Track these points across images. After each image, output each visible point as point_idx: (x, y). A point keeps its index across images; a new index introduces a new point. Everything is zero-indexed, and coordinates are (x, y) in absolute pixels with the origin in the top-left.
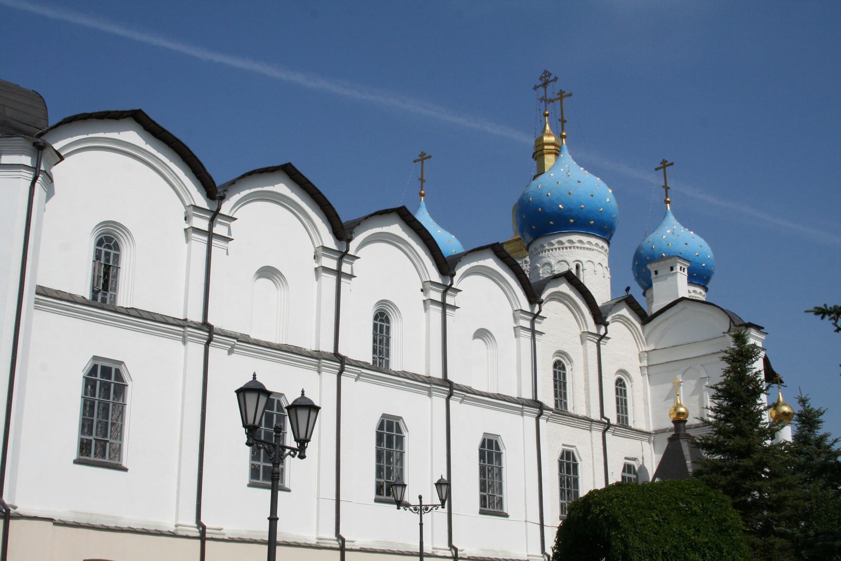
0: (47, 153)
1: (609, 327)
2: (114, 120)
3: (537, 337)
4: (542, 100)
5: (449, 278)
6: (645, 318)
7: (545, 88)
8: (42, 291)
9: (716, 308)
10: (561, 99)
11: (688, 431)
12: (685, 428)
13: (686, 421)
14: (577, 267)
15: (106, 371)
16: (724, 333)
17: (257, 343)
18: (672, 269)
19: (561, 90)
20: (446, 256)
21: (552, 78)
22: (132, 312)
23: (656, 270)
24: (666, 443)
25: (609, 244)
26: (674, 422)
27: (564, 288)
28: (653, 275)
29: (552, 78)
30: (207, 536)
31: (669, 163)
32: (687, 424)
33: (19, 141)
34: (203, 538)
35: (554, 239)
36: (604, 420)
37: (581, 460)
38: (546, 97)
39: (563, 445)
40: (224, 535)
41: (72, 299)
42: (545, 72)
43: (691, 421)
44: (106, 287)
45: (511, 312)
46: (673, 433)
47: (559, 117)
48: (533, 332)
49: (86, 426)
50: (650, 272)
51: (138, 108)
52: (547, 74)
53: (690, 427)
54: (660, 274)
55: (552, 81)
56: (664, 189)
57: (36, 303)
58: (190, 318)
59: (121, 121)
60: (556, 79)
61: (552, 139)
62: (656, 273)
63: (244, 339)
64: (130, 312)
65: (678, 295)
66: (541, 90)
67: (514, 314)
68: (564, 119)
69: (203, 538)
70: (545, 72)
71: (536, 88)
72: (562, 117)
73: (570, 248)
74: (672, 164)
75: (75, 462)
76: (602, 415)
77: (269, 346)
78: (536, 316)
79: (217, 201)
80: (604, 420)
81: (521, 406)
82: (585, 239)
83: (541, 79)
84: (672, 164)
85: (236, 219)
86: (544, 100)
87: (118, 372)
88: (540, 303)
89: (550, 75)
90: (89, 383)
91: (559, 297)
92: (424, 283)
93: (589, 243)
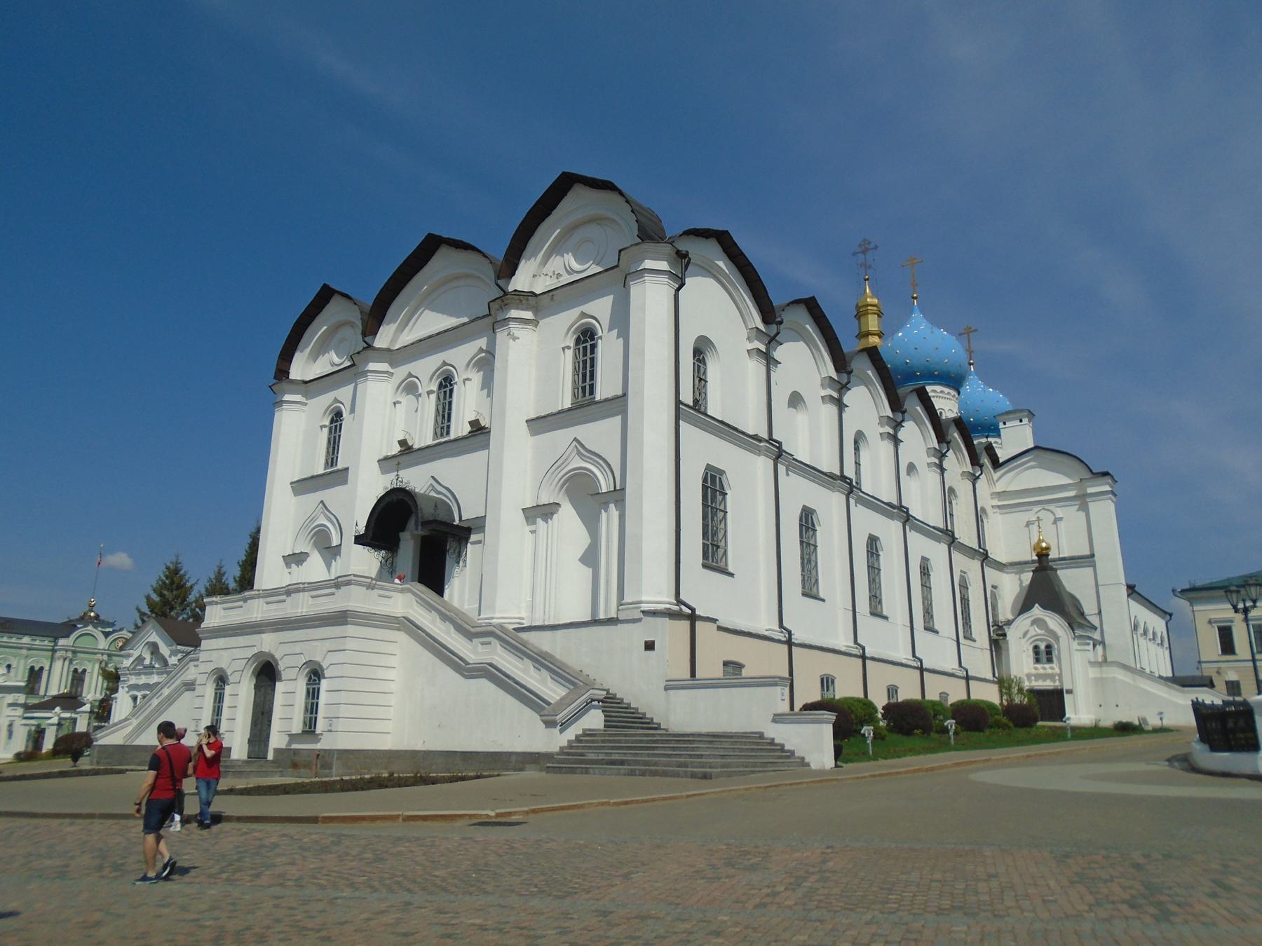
2: (704, 239)
4: (861, 265)
5: (901, 415)
6: (996, 464)
7: (865, 254)
12: (1048, 561)
13: (1048, 555)
18: (1021, 421)
21: (871, 247)
24: (1032, 573)
25: (959, 393)
26: (1037, 555)
28: (1001, 425)
29: (871, 247)
31: (973, 329)
32: (1050, 557)
33: (667, 248)
36: (981, 550)
37: (970, 585)
42: (864, 240)
45: (925, 450)
46: (1037, 565)
51: (726, 229)
53: (1054, 560)
55: (872, 249)
59: (709, 239)
60: (876, 247)
61: (875, 301)
62: (1005, 423)
66: (861, 256)
69: (790, 643)
70: (864, 240)
71: (854, 254)
74: (975, 331)
76: (980, 547)
80: (981, 550)
81: (940, 534)
82: (946, 390)
83: (860, 246)
84: (975, 331)
89: (870, 243)
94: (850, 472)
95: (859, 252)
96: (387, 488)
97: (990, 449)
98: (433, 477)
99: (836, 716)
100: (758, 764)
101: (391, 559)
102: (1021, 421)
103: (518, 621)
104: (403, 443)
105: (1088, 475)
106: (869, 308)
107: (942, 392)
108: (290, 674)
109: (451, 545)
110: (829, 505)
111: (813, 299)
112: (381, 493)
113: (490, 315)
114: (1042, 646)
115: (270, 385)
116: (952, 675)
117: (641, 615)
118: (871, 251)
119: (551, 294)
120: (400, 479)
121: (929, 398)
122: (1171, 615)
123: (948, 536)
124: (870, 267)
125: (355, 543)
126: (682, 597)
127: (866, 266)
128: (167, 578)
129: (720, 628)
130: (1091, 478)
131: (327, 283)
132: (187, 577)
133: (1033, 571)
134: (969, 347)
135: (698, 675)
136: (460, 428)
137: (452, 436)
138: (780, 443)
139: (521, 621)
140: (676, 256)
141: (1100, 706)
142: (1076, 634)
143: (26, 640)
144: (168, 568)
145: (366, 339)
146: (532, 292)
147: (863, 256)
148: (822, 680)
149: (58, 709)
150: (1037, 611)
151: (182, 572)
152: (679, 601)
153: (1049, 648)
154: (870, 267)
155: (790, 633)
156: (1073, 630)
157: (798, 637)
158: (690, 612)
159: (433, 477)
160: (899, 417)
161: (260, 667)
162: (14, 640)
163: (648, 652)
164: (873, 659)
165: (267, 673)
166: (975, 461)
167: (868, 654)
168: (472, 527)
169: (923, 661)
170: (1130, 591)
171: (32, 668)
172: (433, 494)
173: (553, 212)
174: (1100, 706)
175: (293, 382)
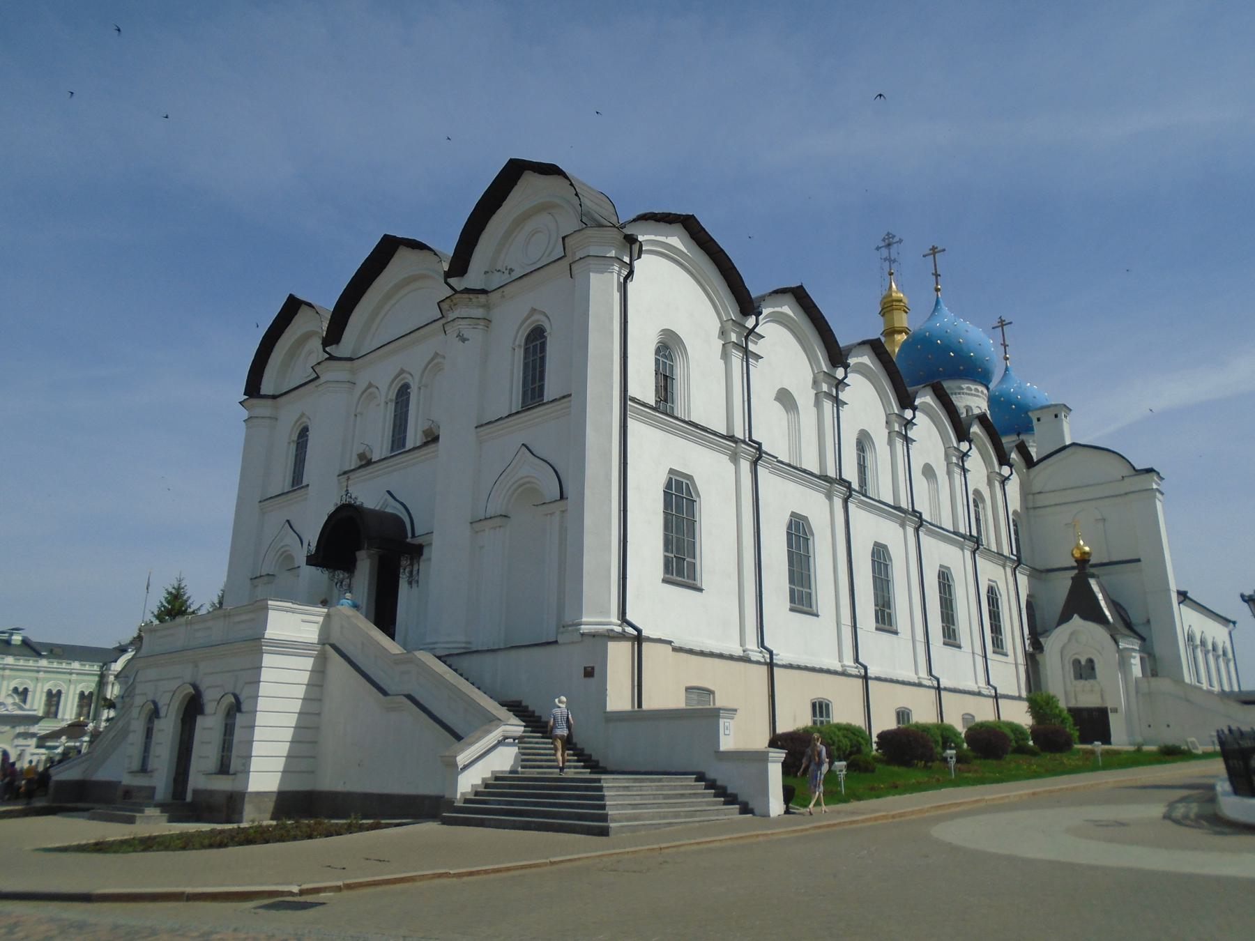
0: (636, 248)
2: (668, 225)
4: (885, 260)
6: (1030, 463)
7: (889, 249)
9: (1112, 454)
10: (934, 254)
11: (1092, 570)
13: (1089, 561)
16: (1123, 477)
19: (933, 246)
23: (1039, 417)
25: (988, 389)
28: (1035, 421)
29: (894, 241)
30: (775, 661)
31: (1006, 322)
32: (1091, 563)
34: (771, 665)
35: (964, 384)
37: (1001, 596)
38: (890, 256)
39: (989, 580)
40: (782, 660)
42: (888, 234)
43: (1093, 561)
47: (934, 272)
50: (1032, 421)
52: (891, 236)
54: (1042, 420)
55: (895, 243)
56: (1003, 347)
59: (673, 225)
60: (900, 241)
65: (1065, 442)
66: (885, 252)
67: (946, 451)
68: (938, 273)
69: (771, 665)
70: (888, 234)
71: (878, 248)
72: (936, 272)
73: (959, 394)
74: (1010, 323)
79: (754, 317)
83: (884, 240)
84: (1010, 323)
85: (764, 337)
86: (889, 260)
89: (894, 236)
92: (888, 416)
94: (850, 474)
95: (882, 247)
96: (337, 505)
97: (1023, 450)
98: (389, 492)
99: (786, 754)
100: (682, 814)
101: (348, 580)
102: (1056, 416)
103: (463, 645)
104: (362, 456)
105: (1129, 472)
106: (894, 303)
108: (209, 707)
109: (404, 562)
111: (801, 288)
112: (332, 509)
113: (443, 317)
114: (1083, 663)
115: (240, 400)
116: (979, 694)
118: (895, 245)
119: (501, 290)
120: (349, 495)
122: (1234, 623)
123: (975, 543)
124: (894, 261)
125: (307, 564)
126: (629, 617)
127: (891, 261)
128: (168, 602)
129: (676, 649)
130: (1135, 475)
131: (293, 293)
132: (188, 603)
133: (1072, 578)
134: (1004, 340)
135: (645, 706)
136: (413, 437)
137: (407, 449)
138: (760, 444)
139: (468, 646)
140: (624, 241)
141: (1150, 726)
142: (1121, 647)
143: (76, 665)
144: (170, 593)
145: (327, 349)
146: (483, 289)
147: (887, 251)
148: (814, 705)
149: (64, 739)
150: (1076, 619)
151: (185, 598)
153: (1091, 661)
154: (894, 261)
155: (771, 653)
156: (1117, 643)
157: (782, 656)
158: (636, 633)
159: (389, 492)
161: (186, 703)
162: (64, 665)
163: (587, 679)
164: (878, 679)
165: (193, 707)
166: (1003, 460)
167: (872, 672)
168: (424, 544)
169: (941, 680)
170: (1182, 598)
171: (82, 694)
172: (389, 510)
173: (504, 204)
174: (1150, 726)
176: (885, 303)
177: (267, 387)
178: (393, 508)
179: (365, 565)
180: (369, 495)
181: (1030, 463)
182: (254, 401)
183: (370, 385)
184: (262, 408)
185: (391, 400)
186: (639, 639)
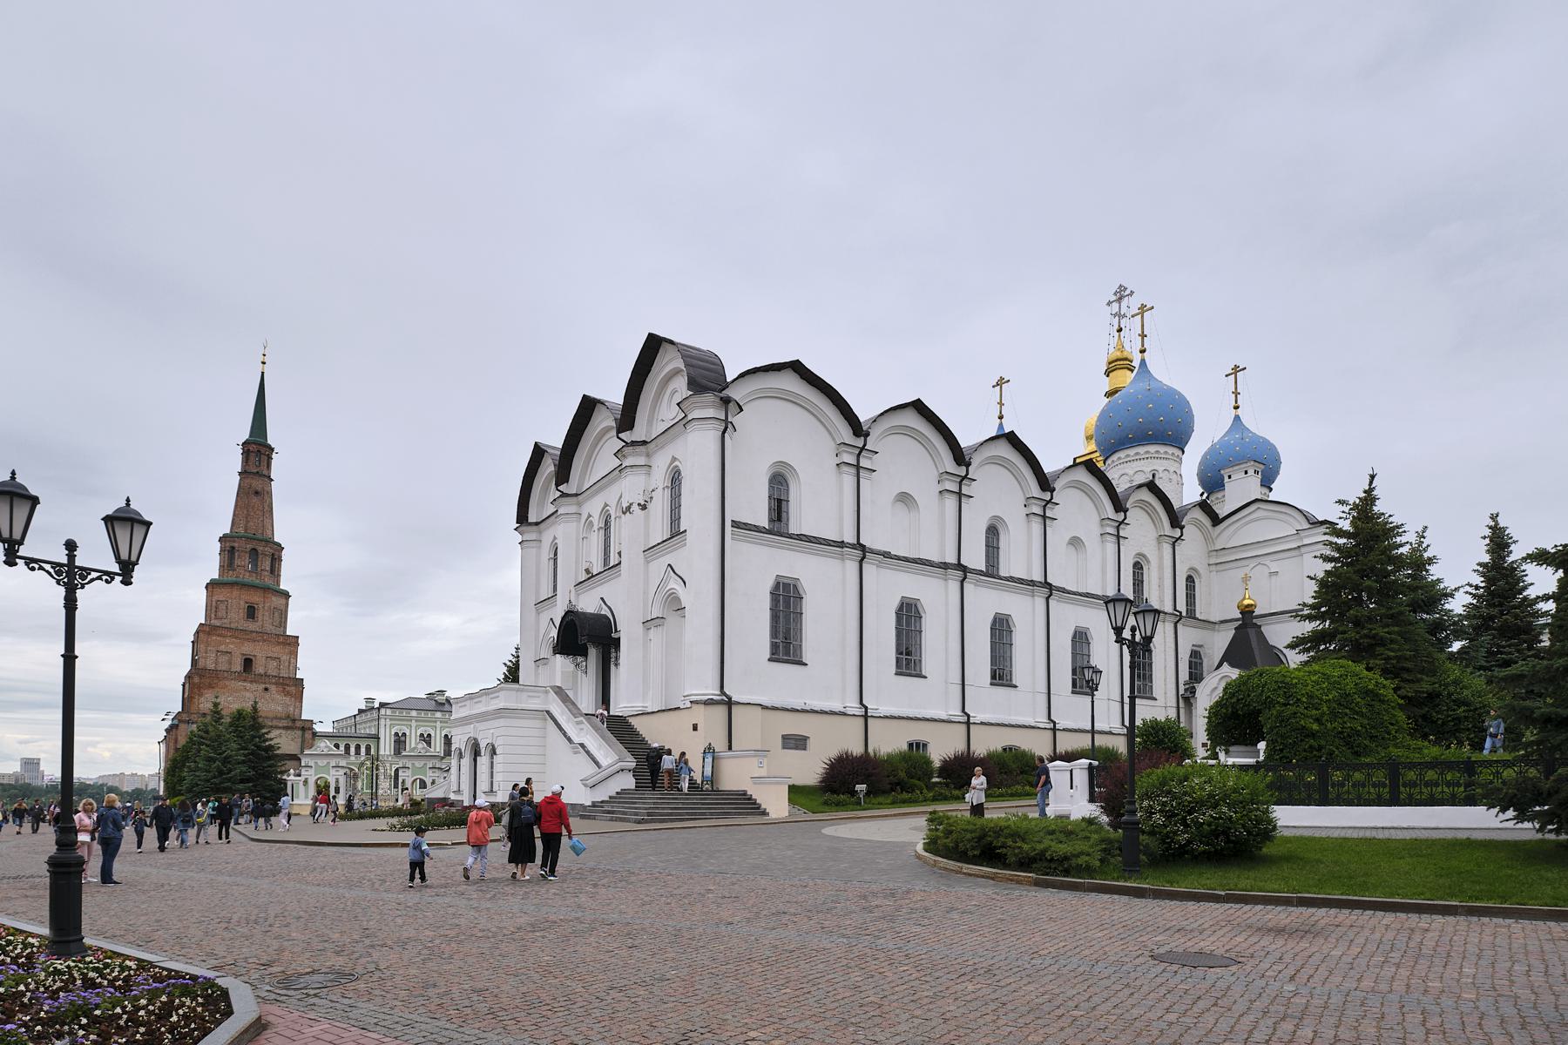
1: (1184, 530)
3: (1121, 540)
5: (1049, 493)
6: (1216, 520)
8: (736, 524)
14: (1154, 476)
15: (786, 586)
17: (898, 558)
20: (1046, 472)
22: (804, 538)
27: (1146, 495)
30: (869, 714)
34: (866, 717)
41: (757, 529)
44: (779, 519)
45: (1098, 519)
48: (1118, 537)
49: (774, 632)
57: (732, 534)
58: (846, 541)
63: (887, 555)
64: (800, 537)
69: (866, 717)
75: (769, 660)
77: (906, 560)
78: (1122, 522)
87: (795, 586)
88: (1125, 511)
90: (774, 595)
91: (1142, 505)
93: (1166, 452)
98: (602, 599)
104: (587, 571)
107: (1157, 452)
110: (935, 596)
117: (689, 705)
121: (1102, 472)
145: (560, 488)
152: (723, 692)
159: (602, 599)
160: (1047, 496)
172: (603, 613)
175: (531, 524)
176: (1110, 363)
177: (532, 518)
178: (605, 612)
179: (593, 652)
180: (588, 604)
181: (1216, 520)
182: (524, 528)
183: (590, 516)
184: (531, 535)
185: (601, 528)
186: (729, 703)
